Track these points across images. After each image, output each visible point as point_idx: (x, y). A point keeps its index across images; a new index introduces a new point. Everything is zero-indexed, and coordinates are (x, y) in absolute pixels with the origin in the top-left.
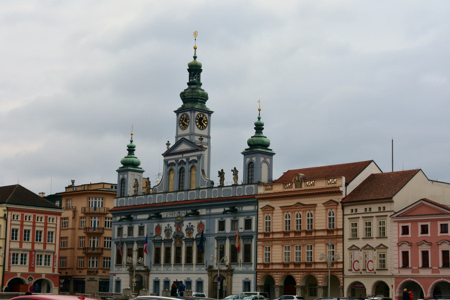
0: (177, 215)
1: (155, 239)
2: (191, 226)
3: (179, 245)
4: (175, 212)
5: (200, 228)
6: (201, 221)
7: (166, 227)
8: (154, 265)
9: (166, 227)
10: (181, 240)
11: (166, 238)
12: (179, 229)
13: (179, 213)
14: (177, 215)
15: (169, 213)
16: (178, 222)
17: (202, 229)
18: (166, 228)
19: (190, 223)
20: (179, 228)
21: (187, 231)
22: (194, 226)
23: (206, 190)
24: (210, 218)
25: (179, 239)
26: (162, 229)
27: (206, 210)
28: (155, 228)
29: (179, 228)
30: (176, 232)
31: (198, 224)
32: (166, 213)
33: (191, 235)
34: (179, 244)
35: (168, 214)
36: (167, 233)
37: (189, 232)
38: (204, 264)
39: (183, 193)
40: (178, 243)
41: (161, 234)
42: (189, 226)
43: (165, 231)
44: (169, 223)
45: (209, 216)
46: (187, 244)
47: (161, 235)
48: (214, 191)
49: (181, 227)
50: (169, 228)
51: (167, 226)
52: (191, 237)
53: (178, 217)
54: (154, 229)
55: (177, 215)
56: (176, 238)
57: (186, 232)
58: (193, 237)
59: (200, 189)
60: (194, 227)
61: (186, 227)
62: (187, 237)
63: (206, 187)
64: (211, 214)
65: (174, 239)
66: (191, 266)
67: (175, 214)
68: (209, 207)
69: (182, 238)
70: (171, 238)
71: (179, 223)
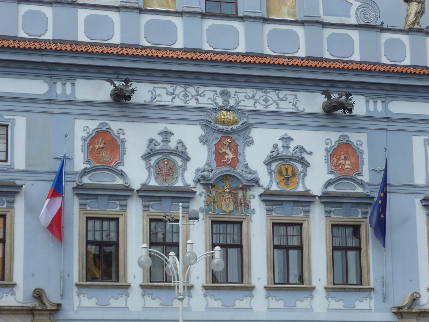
0: (214, 100)
1: (86, 180)
2: (291, 150)
3: (231, 212)
4: (202, 89)
5: (342, 162)
6: (347, 136)
7: (151, 141)
8: (78, 286)
9: (151, 141)
10: (240, 195)
11: (153, 183)
12: (231, 156)
13: (225, 94)
14: (214, 100)
15: (164, 91)
16: (220, 127)
17: (348, 162)
18: (155, 145)
19: (287, 139)
20: (228, 151)
21: (274, 166)
22: (308, 150)
23: (354, 34)
24: (387, 130)
25: (230, 193)
26: (127, 145)
27: (367, 102)
28: (84, 140)
29: (228, 151)
30: (214, 165)
31: (327, 144)
32: (150, 87)
33: (293, 179)
34: (231, 208)
35: (158, 91)
36: (158, 163)
37: (286, 170)
38: (372, 289)
39: (238, 25)
40: (228, 207)
41: (121, 163)
42: (281, 149)
43: (147, 157)
44: (166, 128)
45: (385, 123)
46: (274, 214)
47: (120, 168)
48: (388, 41)
49: (240, 150)
50: (172, 145)
51: (159, 139)
52: (296, 187)
53: (221, 108)
54: (78, 144)
55: (210, 102)
56: (213, 186)
57: (268, 169)
58: (308, 188)
59: (324, 25)
60: (311, 153)
61: (271, 149)
62: (275, 187)
63: (353, 21)
64: (389, 116)
65: (204, 191)
66: (307, 294)
67: (199, 97)
68: (385, 92)
69: (245, 188)
70: (187, 186)
71: (227, 132)
